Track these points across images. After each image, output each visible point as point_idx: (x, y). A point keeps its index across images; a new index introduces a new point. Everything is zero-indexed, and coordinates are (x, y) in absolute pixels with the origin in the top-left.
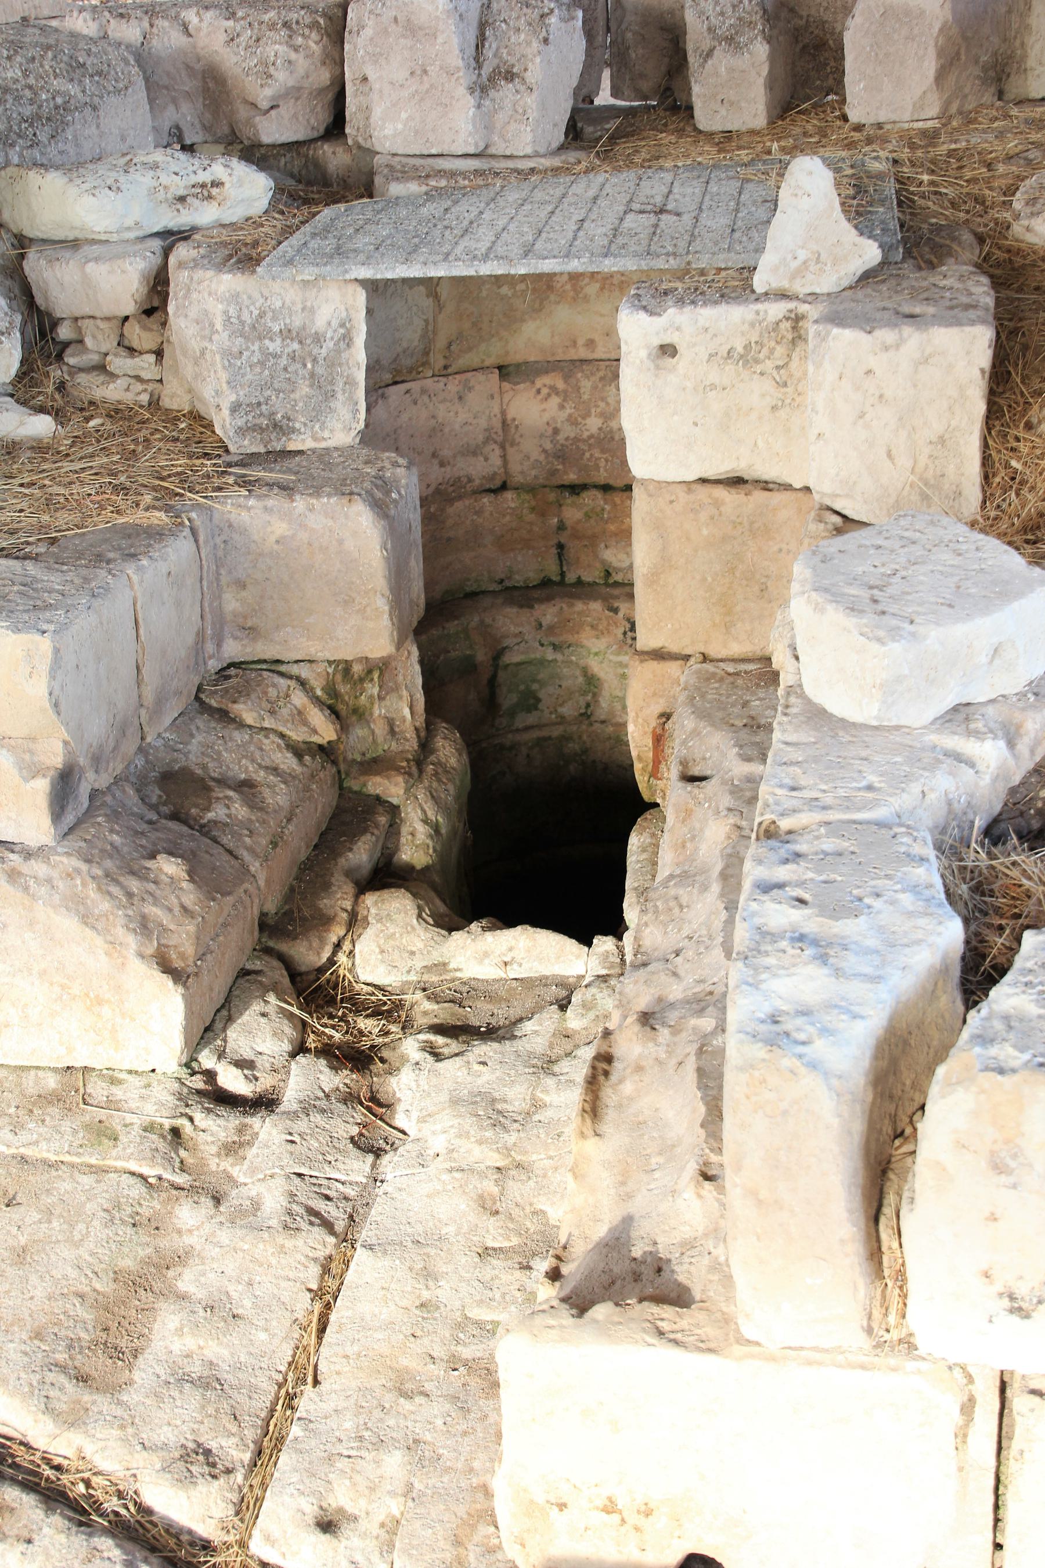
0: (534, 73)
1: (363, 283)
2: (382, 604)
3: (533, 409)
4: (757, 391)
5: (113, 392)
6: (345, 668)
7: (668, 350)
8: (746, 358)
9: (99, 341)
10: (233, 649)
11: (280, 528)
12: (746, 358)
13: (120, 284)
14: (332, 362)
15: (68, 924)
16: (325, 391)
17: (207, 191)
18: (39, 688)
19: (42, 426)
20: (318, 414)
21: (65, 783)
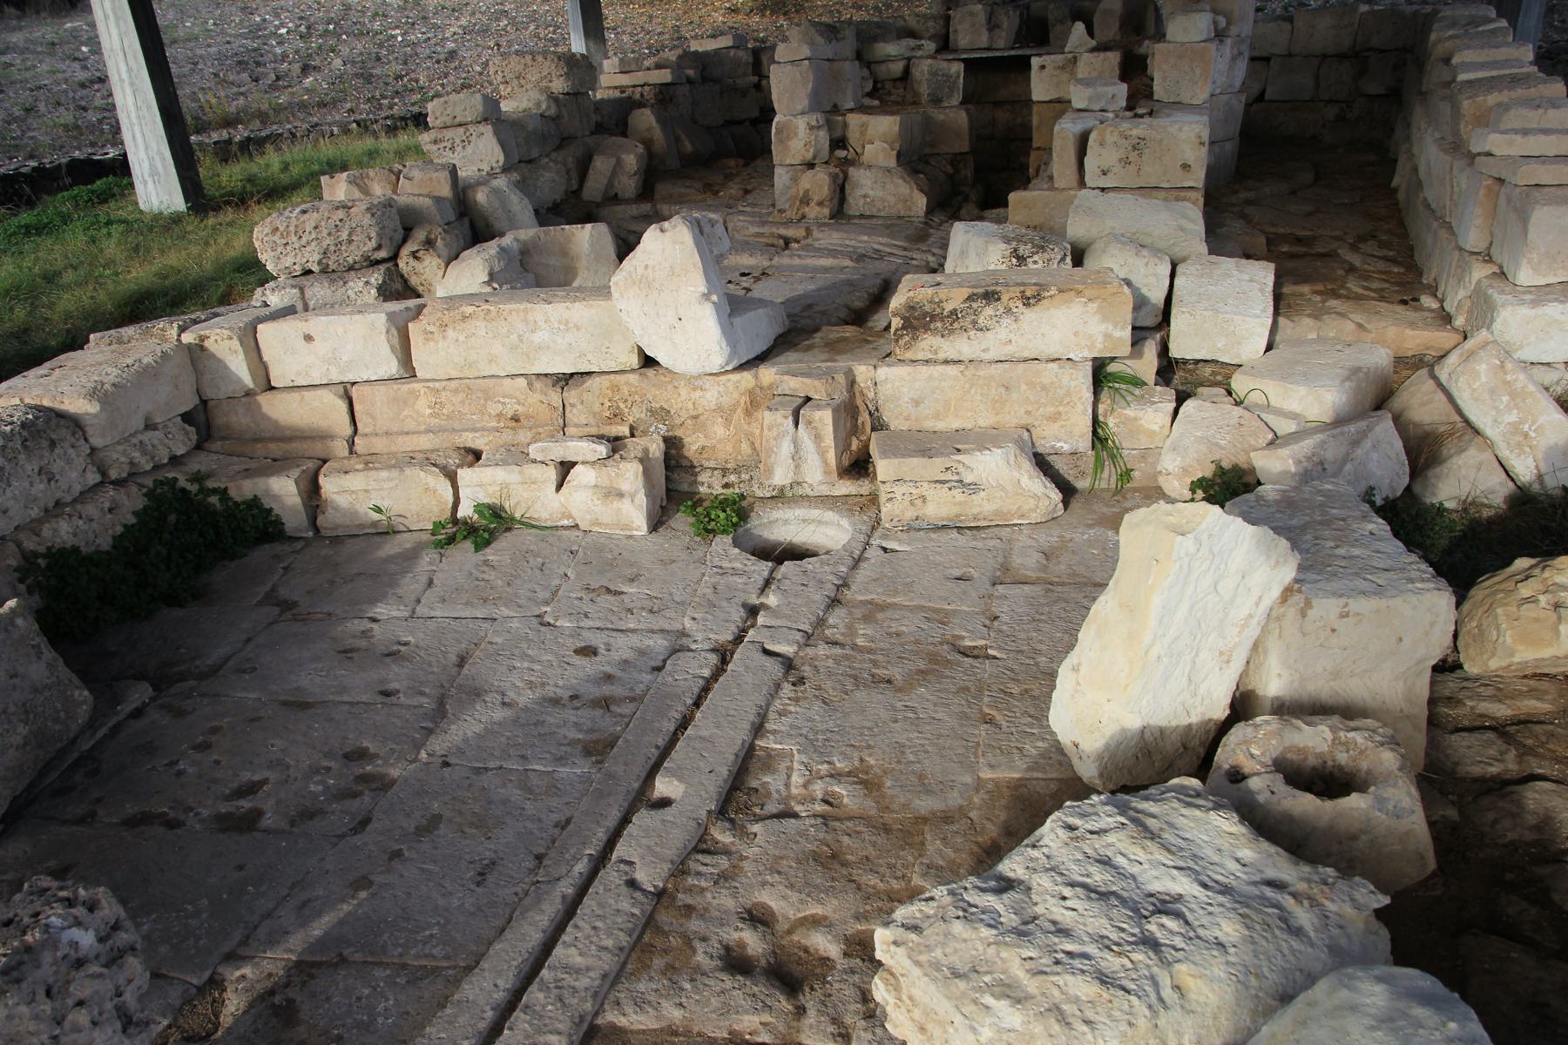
0: (1005, 25)
1: (963, 60)
2: (967, 137)
3: (1002, 116)
4: (1065, 76)
5: (893, 98)
6: (956, 154)
7: (1043, 67)
8: (1063, 68)
9: (888, 86)
10: (927, 151)
11: (942, 117)
12: (1063, 68)
13: (897, 68)
14: (955, 82)
15: (900, 181)
16: (952, 90)
17: (919, 47)
18: (897, 128)
19: (876, 103)
20: (950, 96)
21: (899, 155)
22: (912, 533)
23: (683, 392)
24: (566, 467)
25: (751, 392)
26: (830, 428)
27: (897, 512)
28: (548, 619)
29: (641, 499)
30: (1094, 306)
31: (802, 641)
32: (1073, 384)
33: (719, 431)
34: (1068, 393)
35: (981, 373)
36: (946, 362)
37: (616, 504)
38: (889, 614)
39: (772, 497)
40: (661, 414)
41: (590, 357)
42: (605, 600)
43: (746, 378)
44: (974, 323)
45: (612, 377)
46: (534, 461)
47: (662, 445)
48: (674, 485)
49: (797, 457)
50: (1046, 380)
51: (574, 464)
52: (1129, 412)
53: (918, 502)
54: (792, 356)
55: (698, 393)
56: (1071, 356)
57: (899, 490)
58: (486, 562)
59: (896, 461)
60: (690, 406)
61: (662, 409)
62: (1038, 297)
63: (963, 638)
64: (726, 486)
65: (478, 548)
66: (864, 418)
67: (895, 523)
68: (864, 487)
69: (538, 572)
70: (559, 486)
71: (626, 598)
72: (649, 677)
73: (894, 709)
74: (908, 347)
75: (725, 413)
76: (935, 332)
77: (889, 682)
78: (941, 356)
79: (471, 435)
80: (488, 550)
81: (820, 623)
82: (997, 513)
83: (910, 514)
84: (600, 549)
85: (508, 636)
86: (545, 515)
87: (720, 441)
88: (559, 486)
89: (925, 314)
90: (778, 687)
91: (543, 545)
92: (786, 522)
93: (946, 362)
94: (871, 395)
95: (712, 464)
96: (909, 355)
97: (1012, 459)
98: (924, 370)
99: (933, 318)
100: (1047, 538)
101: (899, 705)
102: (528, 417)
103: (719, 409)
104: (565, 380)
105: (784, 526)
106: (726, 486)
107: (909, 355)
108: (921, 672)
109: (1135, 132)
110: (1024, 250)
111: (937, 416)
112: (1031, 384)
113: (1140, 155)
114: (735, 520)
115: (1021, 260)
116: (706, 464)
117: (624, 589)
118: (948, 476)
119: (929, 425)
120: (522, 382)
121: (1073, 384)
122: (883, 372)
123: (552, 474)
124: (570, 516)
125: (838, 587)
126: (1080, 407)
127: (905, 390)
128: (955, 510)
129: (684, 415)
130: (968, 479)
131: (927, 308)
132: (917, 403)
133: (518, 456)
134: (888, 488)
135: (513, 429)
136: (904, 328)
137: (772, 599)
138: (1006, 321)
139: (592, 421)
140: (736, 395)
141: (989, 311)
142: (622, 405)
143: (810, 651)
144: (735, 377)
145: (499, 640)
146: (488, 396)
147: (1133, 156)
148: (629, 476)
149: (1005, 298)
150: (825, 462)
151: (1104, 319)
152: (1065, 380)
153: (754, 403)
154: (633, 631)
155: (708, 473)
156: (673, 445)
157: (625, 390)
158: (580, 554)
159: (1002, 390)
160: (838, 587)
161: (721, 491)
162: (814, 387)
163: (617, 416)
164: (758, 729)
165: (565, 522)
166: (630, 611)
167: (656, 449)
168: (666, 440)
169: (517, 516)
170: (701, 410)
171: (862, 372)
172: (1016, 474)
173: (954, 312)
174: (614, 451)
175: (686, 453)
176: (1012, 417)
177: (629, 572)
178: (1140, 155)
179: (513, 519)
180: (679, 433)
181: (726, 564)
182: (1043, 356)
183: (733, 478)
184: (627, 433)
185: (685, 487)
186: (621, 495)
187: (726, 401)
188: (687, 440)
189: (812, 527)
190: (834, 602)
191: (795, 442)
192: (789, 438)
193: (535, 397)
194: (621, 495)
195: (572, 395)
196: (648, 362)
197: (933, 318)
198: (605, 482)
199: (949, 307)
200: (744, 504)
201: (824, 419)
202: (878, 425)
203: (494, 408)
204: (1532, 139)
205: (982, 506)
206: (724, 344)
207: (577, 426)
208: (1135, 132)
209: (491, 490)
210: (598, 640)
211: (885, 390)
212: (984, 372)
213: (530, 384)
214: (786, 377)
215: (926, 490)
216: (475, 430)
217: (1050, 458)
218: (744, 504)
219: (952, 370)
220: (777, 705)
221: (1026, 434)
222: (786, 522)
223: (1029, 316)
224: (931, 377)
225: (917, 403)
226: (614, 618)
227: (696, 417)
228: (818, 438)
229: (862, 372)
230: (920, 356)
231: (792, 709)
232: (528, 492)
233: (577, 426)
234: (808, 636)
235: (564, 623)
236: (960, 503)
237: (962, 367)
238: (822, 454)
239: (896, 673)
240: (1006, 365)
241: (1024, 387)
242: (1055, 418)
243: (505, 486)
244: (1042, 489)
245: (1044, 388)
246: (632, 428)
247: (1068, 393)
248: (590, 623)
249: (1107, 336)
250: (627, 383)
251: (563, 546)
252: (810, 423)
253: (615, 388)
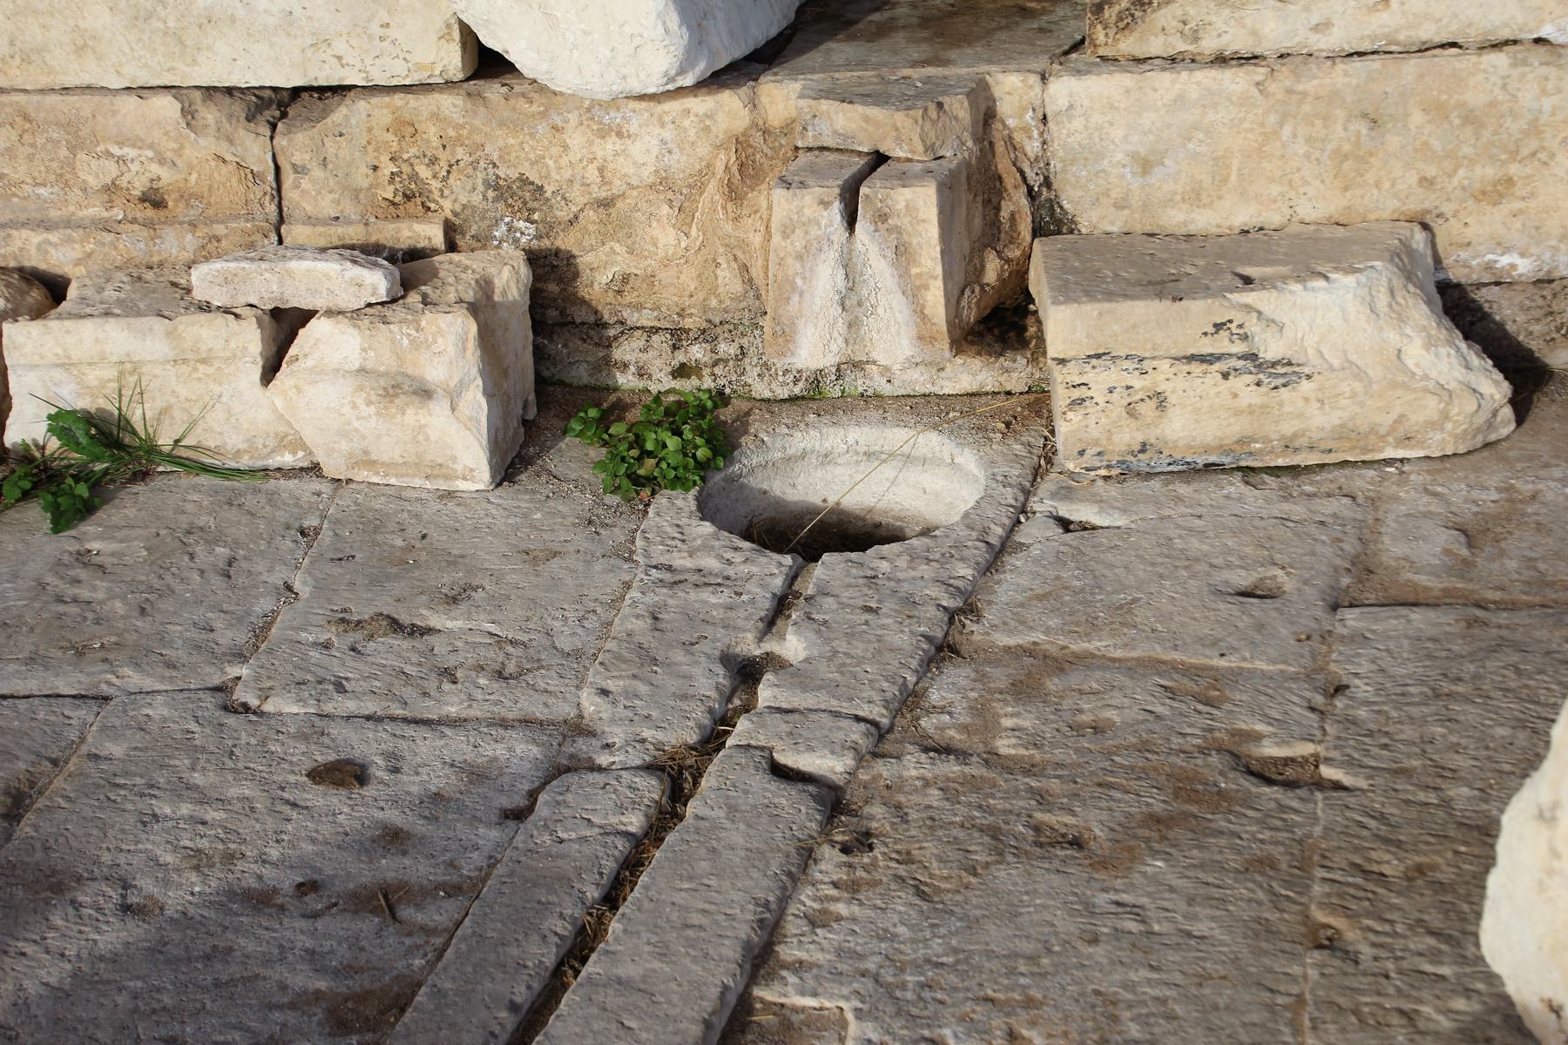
22: (1132, 485)
23: (576, 139)
24: (286, 324)
25: (741, 143)
26: (932, 231)
27: (1095, 433)
28: (244, 695)
29: (476, 402)
31: (864, 743)
32: (1547, 103)
33: (664, 237)
34: (1534, 129)
35: (1309, 86)
36: (1221, 60)
37: (413, 415)
38: (1074, 679)
39: (793, 399)
40: (521, 195)
41: (340, 47)
42: (389, 650)
43: (729, 107)
45: (398, 99)
46: (205, 308)
47: (525, 272)
48: (557, 371)
49: (851, 300)
50: (1474, 97)
51: (304, 317)
53: (1147, 409)
54: (839, 50)
55: (612, 144)
56: (1546, 31)
57: (1100, 379)
58: (83, 558)
59: (1091, 309)
60: (592, 174)
61: (524, 181)
63: (1257, 737)
64: (682, 371)
65: (61, 521)
66: (1016, 203)
67: (1088, 460)
68: (1013, 373)
69: (217, 581)
70: (271, 370)
71: (439, 644)
72: (495, 834)
73: (1090, 909)
74: (1126, 23)
75: (677, 193)
77: (1077, 843)
78: (1209, 45)
79: (36, 238)
80: (88, 527)
81: (910, 700)
82: (1344, 433)
83: (1126, 437)
84: (374, 524)
85: (138, 739)
86: (234, 441)
87: (666, 262)
88: (271, 370)
90: (807, 855)
91: (231, 514)
92: (827, 458)
93: (1221, 60)
94: (1032, 147)
95: (646, 318)
96: (1128, 45)
97: (1383, 299)
98: (1165, 83)
100: (1475, 494)
101: (1102, 899)
102: (185, 196)
103: (663, 183)
104: (278, 106)
105: (822, 468)
106: (682, 371)
107: (1128, 45)
108: (1154, 820)
111: (1195, 197)
112: (1437, 111)
114: (702, 453)
116: (633, 318)
117: (435, 621)
118: (1222, 344)
119: (1176, 218)
120: (167, 106)
121: (1547, 103)
122: (1065, 89)
123: (251, 340)
124: (298, 444)
125: (952, 615)
127: (1117, 133)
128: (1234, 428)
129: (578, 197)
130: (1271, 349)
132: (1145, 165)
133: (161, 293)
134: (1072, 374)
135: (149, 225)
137: (793, 645)
139: (350, 209)
140: (704, 149)
142: (424, 172)
143: (884, 770)
144: (701, 104)
145: (116, 750)
146: (78, 139)
148: (445, 345)
150: (921, 314)
152: (1527, 96)
153: (748, 168)
154: (457, 723)
155: (638, 341)
156: (551, 271)
157: (432, 132)
158: (326, 536)
159: (1363, 128)
160: (952, 615)
161: (668, 383)
162: (895, 129)
163: (412, 199)
164: (761, 959)
165: (287, 459)
166: (449, 674)
167: (510, 280)
168: (535, 259)
169: (164, 441)
170: (618, 186)
171: (1013, 89)
172: (1392, 337)
174: (407, 284)
175: (584, 292)
176: (1387, 193)
177: (450, 579)
179: (152, 450)
180: (565, 242)
181: (681, 561)
182: (1472, 36)
183: (697, 352)
184: (439, 240)
185: (581, 374)
186: (425, 393)
187: (681, 164)
188: (585, 260)
189: (888, 471)
190: (943, 651)
191: (848, 265)
192: (832, 255)
193: (201, 148)
194: (425, 393)
195: (297, 144)
196: (487, 64)
198: (383, 359)
200: (726, 414)
201: (918, 206)
202: (1051, 221)
203: (95, 172)
205: (1306, 417)
206: (674, 20)
207: (311, 221)
209: (93, 376)
210: (367, 745)
211: (1067, 135)
212: (1318, 81)
213: (188, 113)
214: (825, 105)
215: (1164, 377)
216: (46, 225)
217: (1482, 296)
218: (726, 414)
219: (1235, 81)
220: (806, 899)
221: (1419, 239)
222: (827, 458)
224: (1180, 101)
225: (1145, 165)
226: (409, 693)
227: (606, 204)
228: (902, 253)
229: (1013, 89)
230: (1156, 46)
231: (841, 908)
232: (194, 385)
233: (311, 221)
234: (880, 733)
235: (284, 705)
236: (1251, 410)
237: (1260, 73)
238: (913, 292)
239: (1094, 822)
240: (1375, 64)
241: (1417, 118)
242: (1498, 191)
243: (129, 367)
244: (1459, 373)
245: (1471, 119)
246: (450, 230)
247: (1534, 129)
248: (351, 705)
250: (435, 117)
251: (282, 516)
252: (883, 217)
253: (406, 129)
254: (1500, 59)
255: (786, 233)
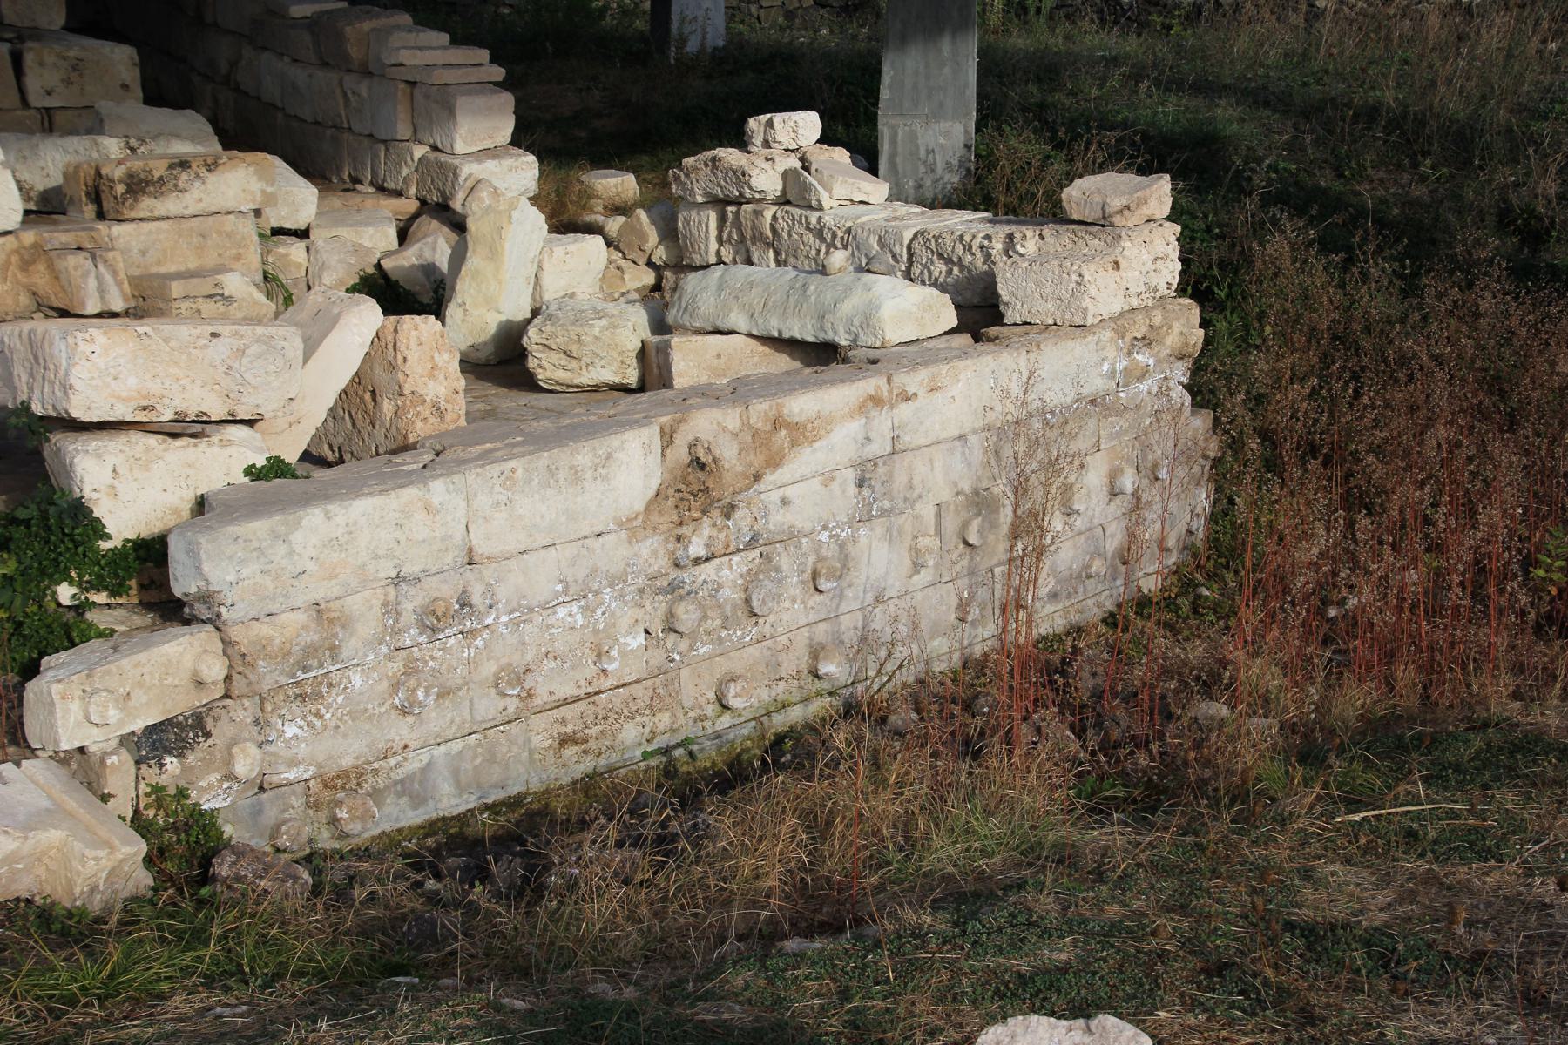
25: (17, 251)
30: (252, 169)
44: (176, 186)
49: (102, 291)
50: (228, 228)
52: (282, 250)
56: (242, 209)
62: (216, 164)
74: (132, 208)
76: (150, 194)
78: (156, 214)
89: (141, 181)
96: (133, 215)
99: (147, 183)
109: (72, 54)
110: (133, 142)
111: (159, 263)
112: (219, 233)
113: (81, 75)
115: (133, 150)
119: (154, 270)
126: (252, 248)
131: (142, 176)
132: (143, 253)
136: (127, 192)
138: (197, 184)
141: (184, 176)
147: (74, 76)
149: (194, 166)
150: (122, 290)
151: (260, 179)
173: (161, 178)
178: (81, 75)
191: (99, 278)
192: (93, 275)
197: (147, 183)
199: (157, 174)
204: (427, 53)
208: (72, 54)
212: (186, 224)
223: (212, 179)
225: (143, 253)
230: (142, 215)
245: (229, 235)
249: (263, 192)
254: (232, 217)
255: (76, 268)
